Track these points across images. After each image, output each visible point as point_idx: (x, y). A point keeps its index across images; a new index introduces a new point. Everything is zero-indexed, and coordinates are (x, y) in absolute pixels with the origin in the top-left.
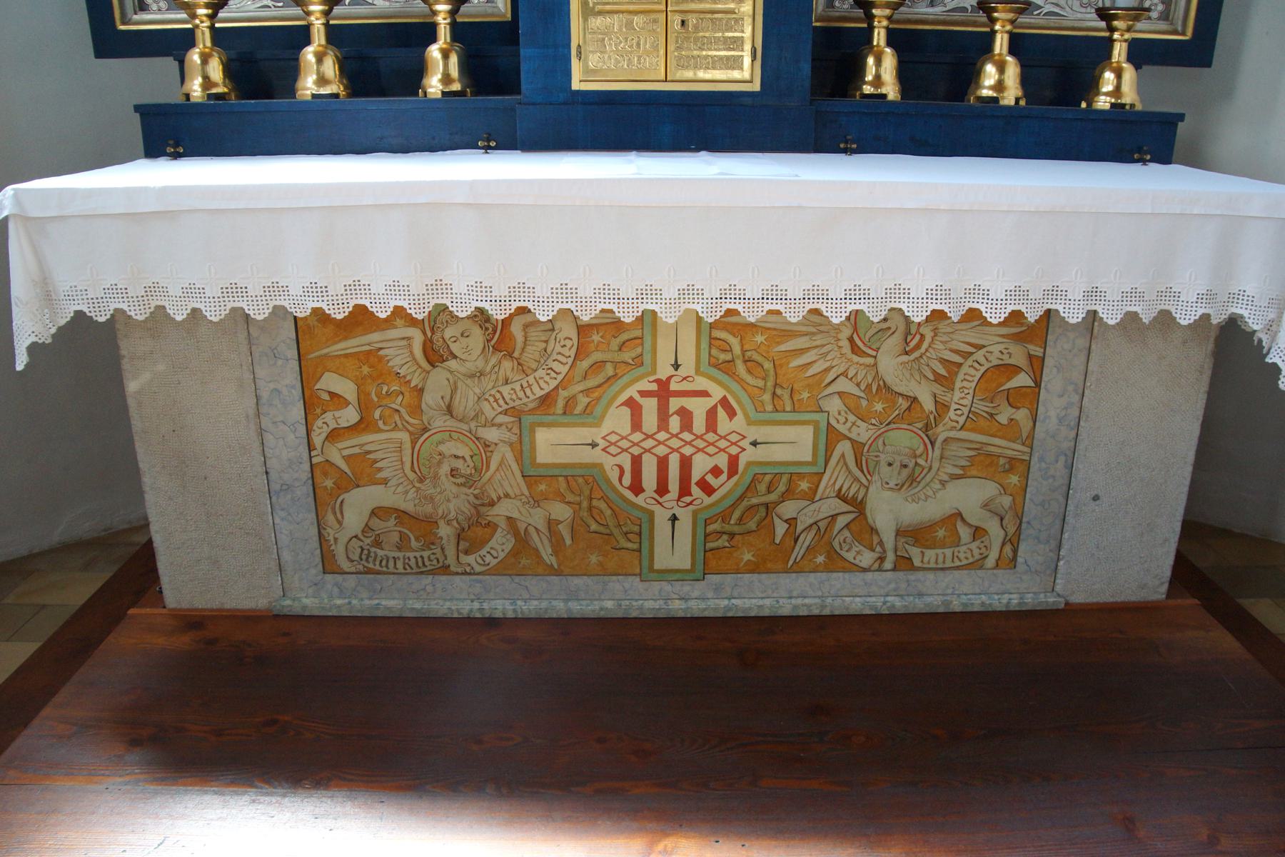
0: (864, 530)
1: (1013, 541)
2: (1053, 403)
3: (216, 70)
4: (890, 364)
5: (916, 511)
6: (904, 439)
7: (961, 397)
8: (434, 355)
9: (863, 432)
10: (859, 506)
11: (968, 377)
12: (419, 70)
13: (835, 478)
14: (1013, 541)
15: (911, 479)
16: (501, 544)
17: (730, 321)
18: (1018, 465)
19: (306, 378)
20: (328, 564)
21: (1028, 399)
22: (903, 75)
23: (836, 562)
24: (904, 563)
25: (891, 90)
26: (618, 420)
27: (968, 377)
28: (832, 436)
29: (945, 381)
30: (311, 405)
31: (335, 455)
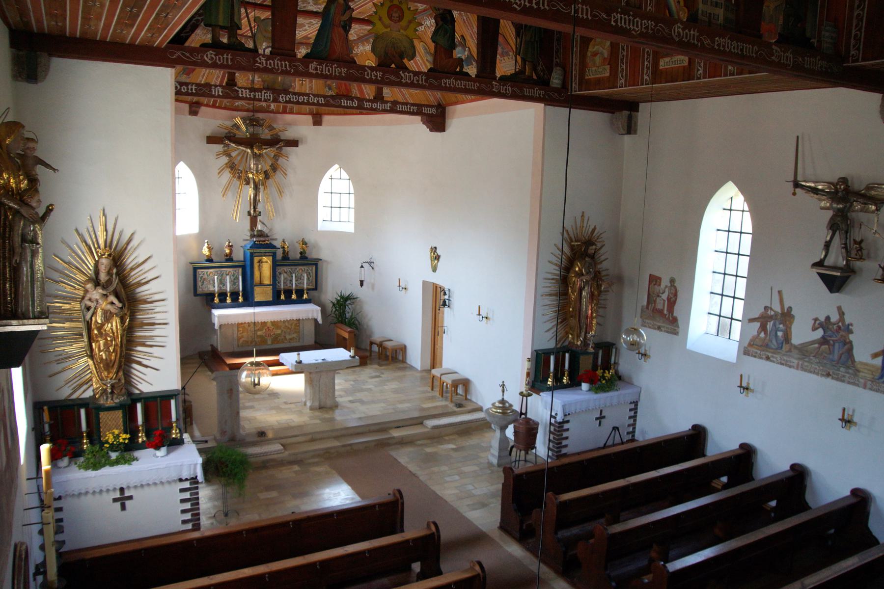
0: (286, 339)
1: (299, 339)
2: (301, 325)
3: (218, 300)
4: (287, 324)
5: (290, 337)
6: (289, 330)
7: (293, 327)
8: (249, 326)
9: (285, 330)
10: (285, 337)
11: (293, 325)
12: (238, 299)
13: (283, 335)
14: (299, 339)
15: (289, 334)
16: (254, 343)
17: (274, 322)
18: (299, 332)
19: (238, 328)
20: (238, 346)
21: (299, 326)
22: (285, 297)
23: (283, 342)
24: (290, 342)
25: (284, 299)
26: (264, 331)
27: (293, 325)
28: (282, 331)
29: (292, 325)
30: (238, 331)
31: (240, 335)
